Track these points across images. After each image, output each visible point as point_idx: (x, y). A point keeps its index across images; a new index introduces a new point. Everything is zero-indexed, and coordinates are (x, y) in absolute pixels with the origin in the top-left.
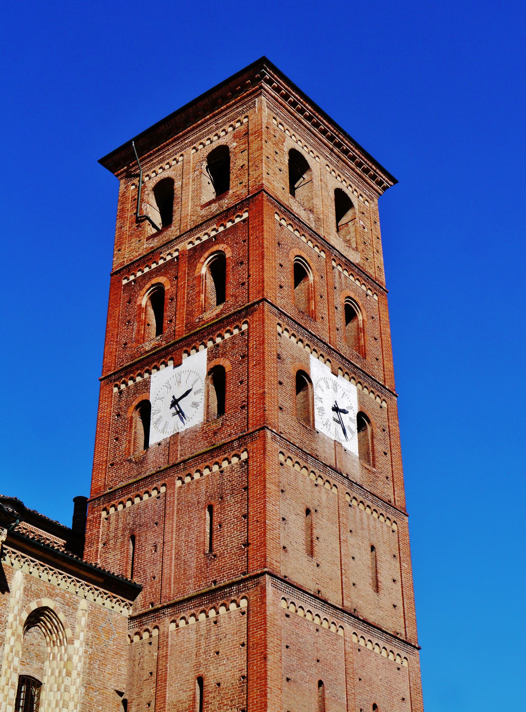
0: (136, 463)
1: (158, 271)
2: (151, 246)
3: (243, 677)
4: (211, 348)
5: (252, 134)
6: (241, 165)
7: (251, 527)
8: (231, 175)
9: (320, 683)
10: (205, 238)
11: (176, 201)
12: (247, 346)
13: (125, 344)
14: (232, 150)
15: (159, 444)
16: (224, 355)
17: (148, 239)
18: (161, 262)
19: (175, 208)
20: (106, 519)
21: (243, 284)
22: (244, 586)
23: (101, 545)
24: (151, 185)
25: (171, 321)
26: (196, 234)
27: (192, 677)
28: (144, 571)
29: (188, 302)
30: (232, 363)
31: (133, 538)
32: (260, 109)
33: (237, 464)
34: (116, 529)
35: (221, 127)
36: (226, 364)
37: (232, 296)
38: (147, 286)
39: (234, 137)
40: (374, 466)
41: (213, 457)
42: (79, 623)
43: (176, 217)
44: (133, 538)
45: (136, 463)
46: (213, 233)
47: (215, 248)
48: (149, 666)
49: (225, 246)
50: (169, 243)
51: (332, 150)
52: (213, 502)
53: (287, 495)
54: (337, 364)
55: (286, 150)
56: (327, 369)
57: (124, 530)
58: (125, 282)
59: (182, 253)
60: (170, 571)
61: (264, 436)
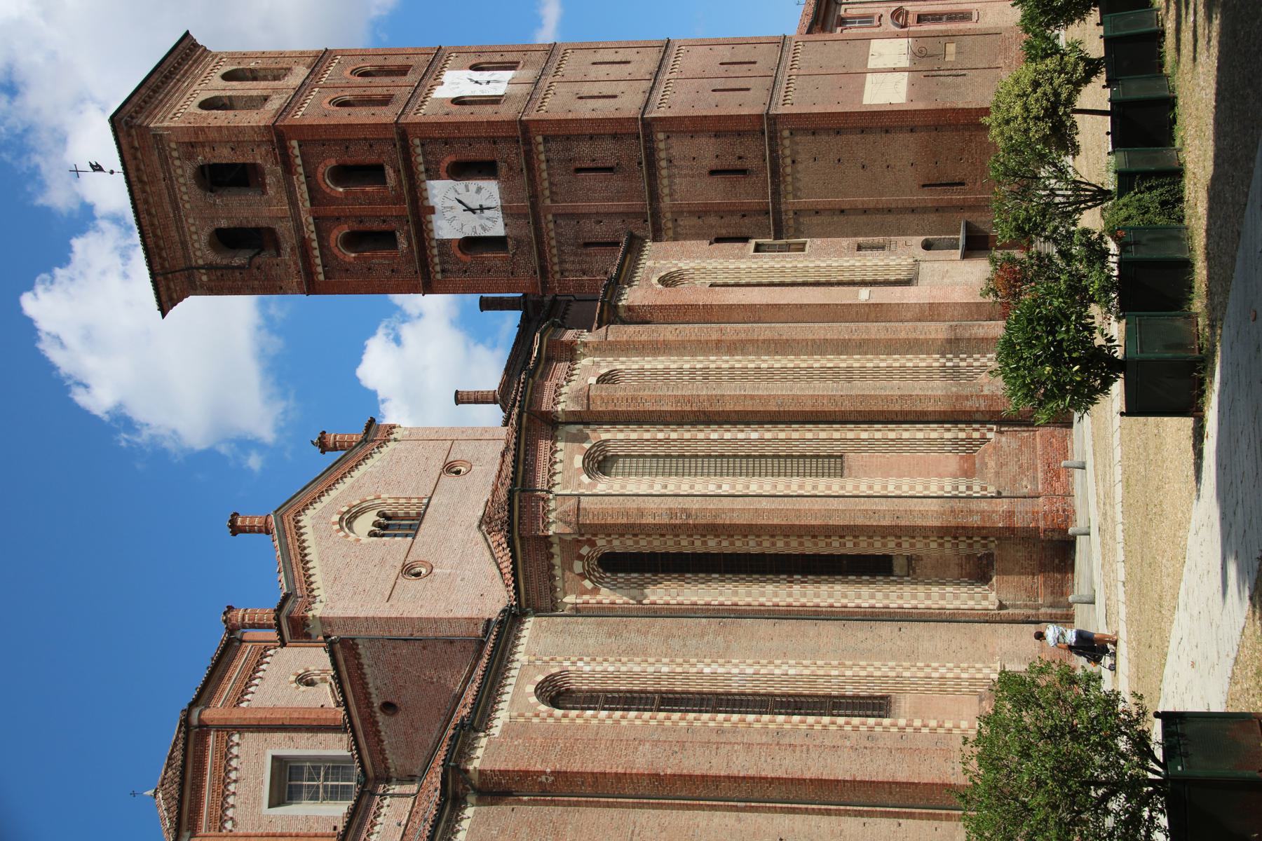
0: (517, 249)
1: (321, 239)
2: (289, 250)
3: (715, 136)
4: (427, 176)
5: (198, 138)
6: (230, 150)
7: (602, 132)
8: (238, 162)
9: (714, 91)
10: (304, 187)
11: (245, 224)
12: (436, 139)
13: (393, 271)
14: (206, 162)
15: (506, 225)
16: (438, 163)
17: (279, 255)
18: (314, 236)
19: (253, 225)
20: (562, 274)
21: (371, 146)
22: (648, 136)
23: (585, 278)
24: (212, 257)
25: (384, 221)
26: (297, 198)
27: (709, 180)
28: (616, 231)
29: (370, 204)
30: (450, 154)
31: (587, 245)
32: (168, 128)
33: (544, 147)
34: (573, 262)
35: (170, 174)
36: (448, 160)
37: (379, 156)
38: (336, 251)
39: (189, 160)
40: (518, 63)
41: (534, 169)
42: (665, 264)
43: (263, 224)
44: (587, 245)
45: (517, 249)
46: (302, 178)
47: (319, 176)
48: (694, 221)
49: (322, 165)
50: (299, 227)
51: (179, 80)
52: (572, 168)
53: (572, 108)
54: (432, 82)
55: (205, 112)
56: (438, 88)
57: (576, 255)
58: (321, 277)
59: (311, 212)
60: (621, 205)
61: (528, 121)
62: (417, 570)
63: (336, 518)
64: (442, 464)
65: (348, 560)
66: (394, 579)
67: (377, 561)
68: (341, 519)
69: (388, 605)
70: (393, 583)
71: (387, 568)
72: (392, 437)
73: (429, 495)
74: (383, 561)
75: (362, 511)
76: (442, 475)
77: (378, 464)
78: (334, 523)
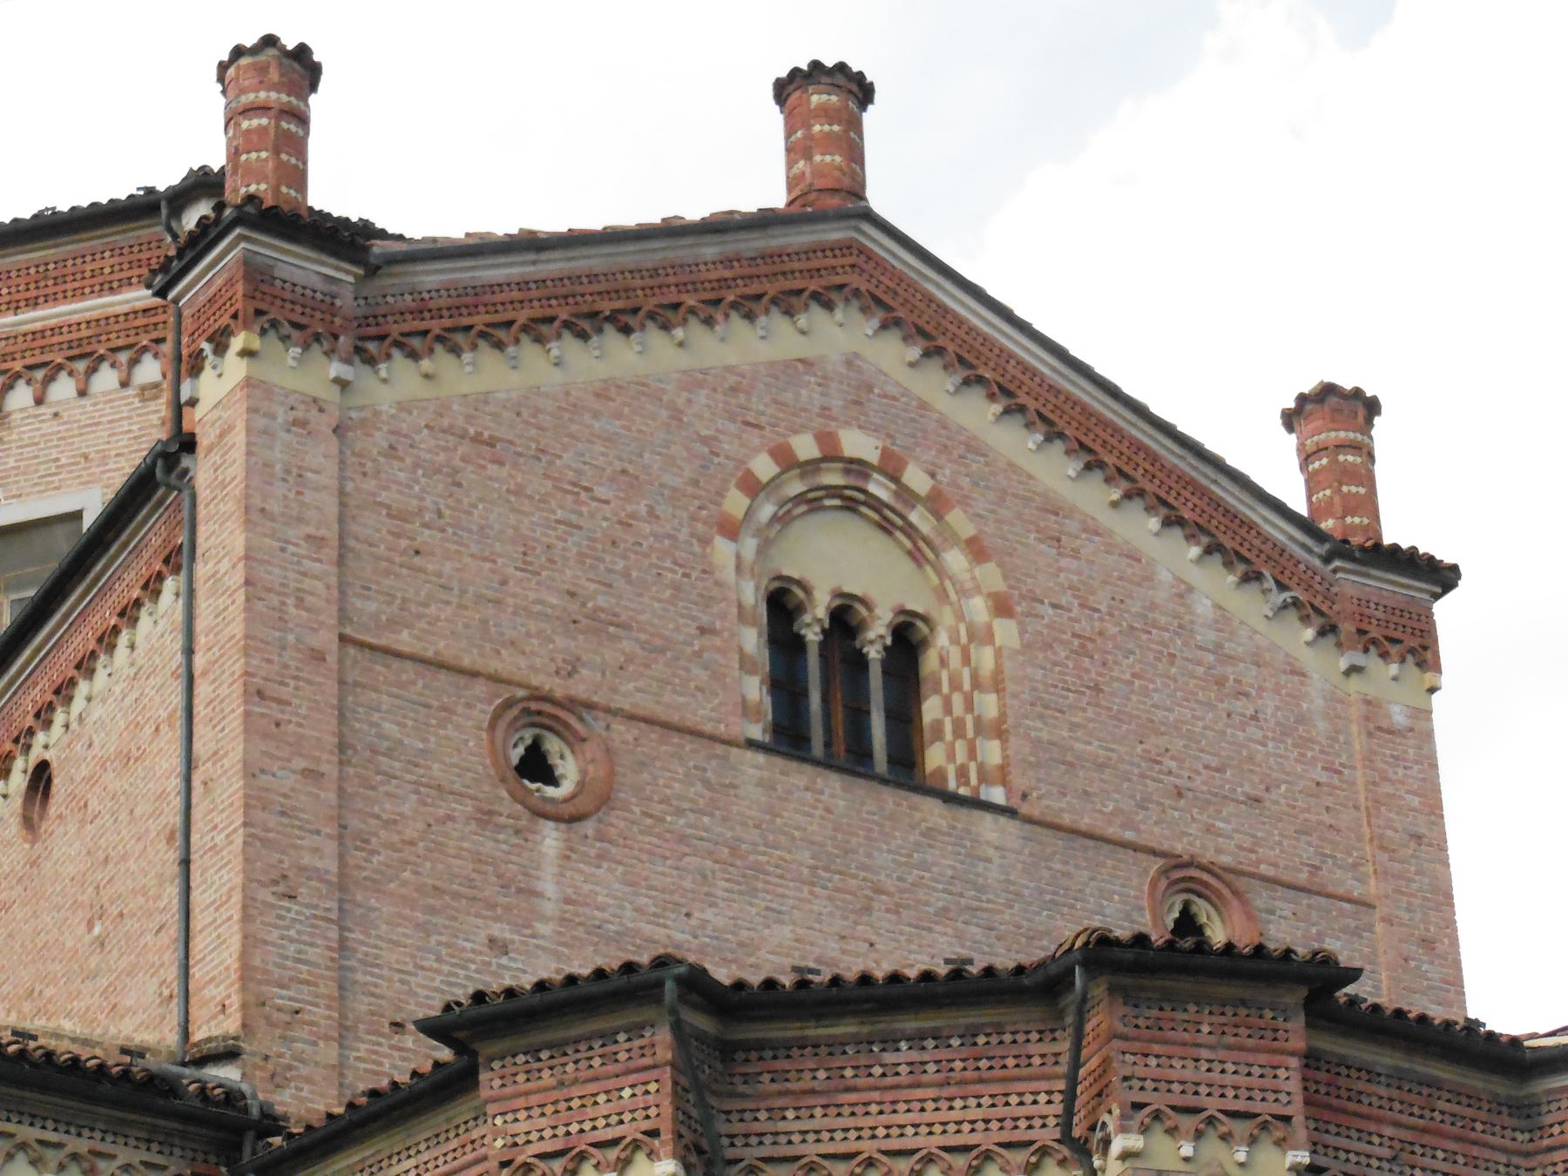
62: (568, 768)
63: (858, 444)
64: (1225, 859)
65: (600, 491)
66: (494, 665)
67: (601, 601)
68: (857, 467)
69: (326, 639)
70: (466, 662)
71: (561, 642)
72: (1358, 658)
73: (1024, 809)
74: (605, 625)
75: (920, 552)
76: (1158, 863)
77: (1203, 607)
78: (827, 440)
